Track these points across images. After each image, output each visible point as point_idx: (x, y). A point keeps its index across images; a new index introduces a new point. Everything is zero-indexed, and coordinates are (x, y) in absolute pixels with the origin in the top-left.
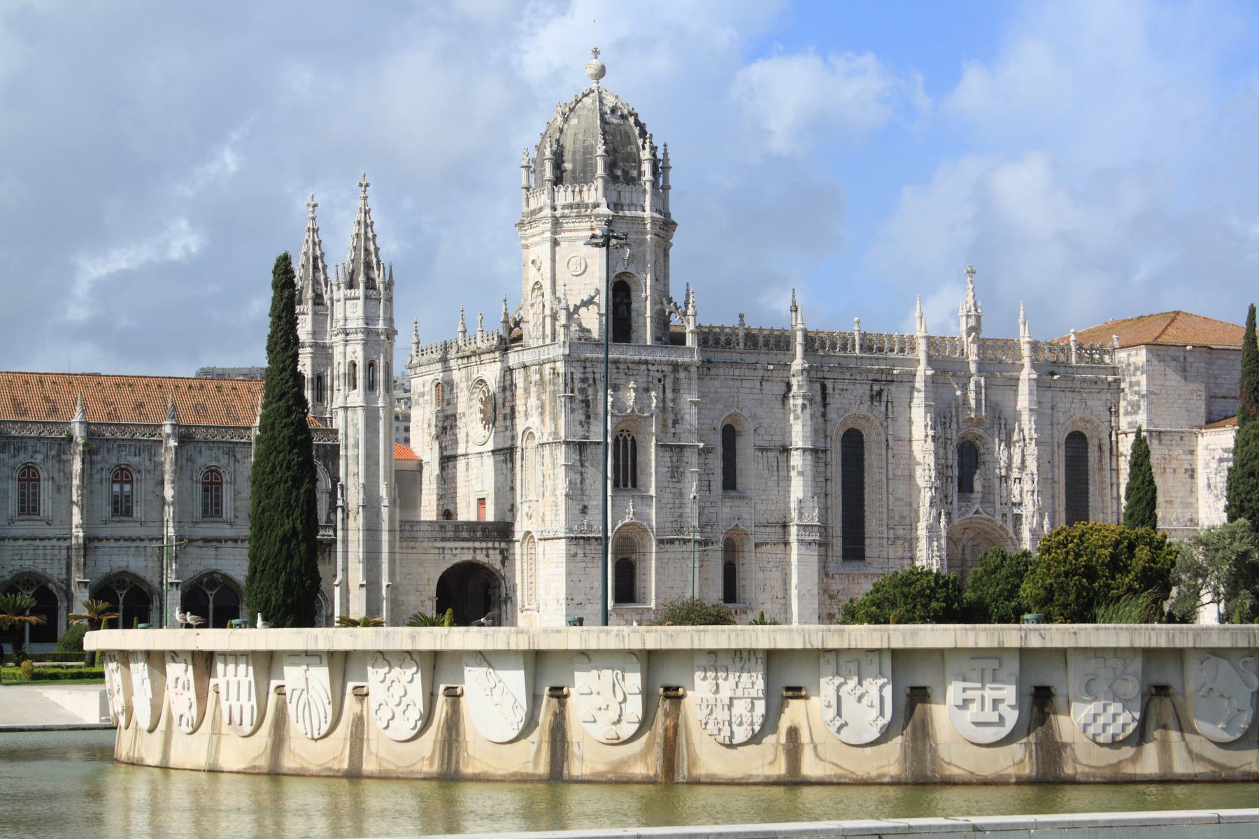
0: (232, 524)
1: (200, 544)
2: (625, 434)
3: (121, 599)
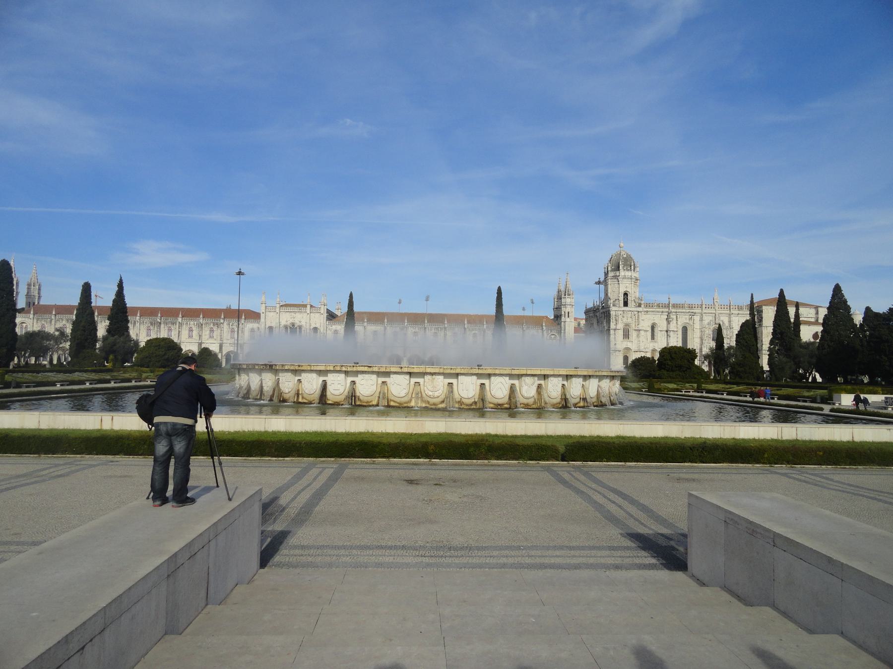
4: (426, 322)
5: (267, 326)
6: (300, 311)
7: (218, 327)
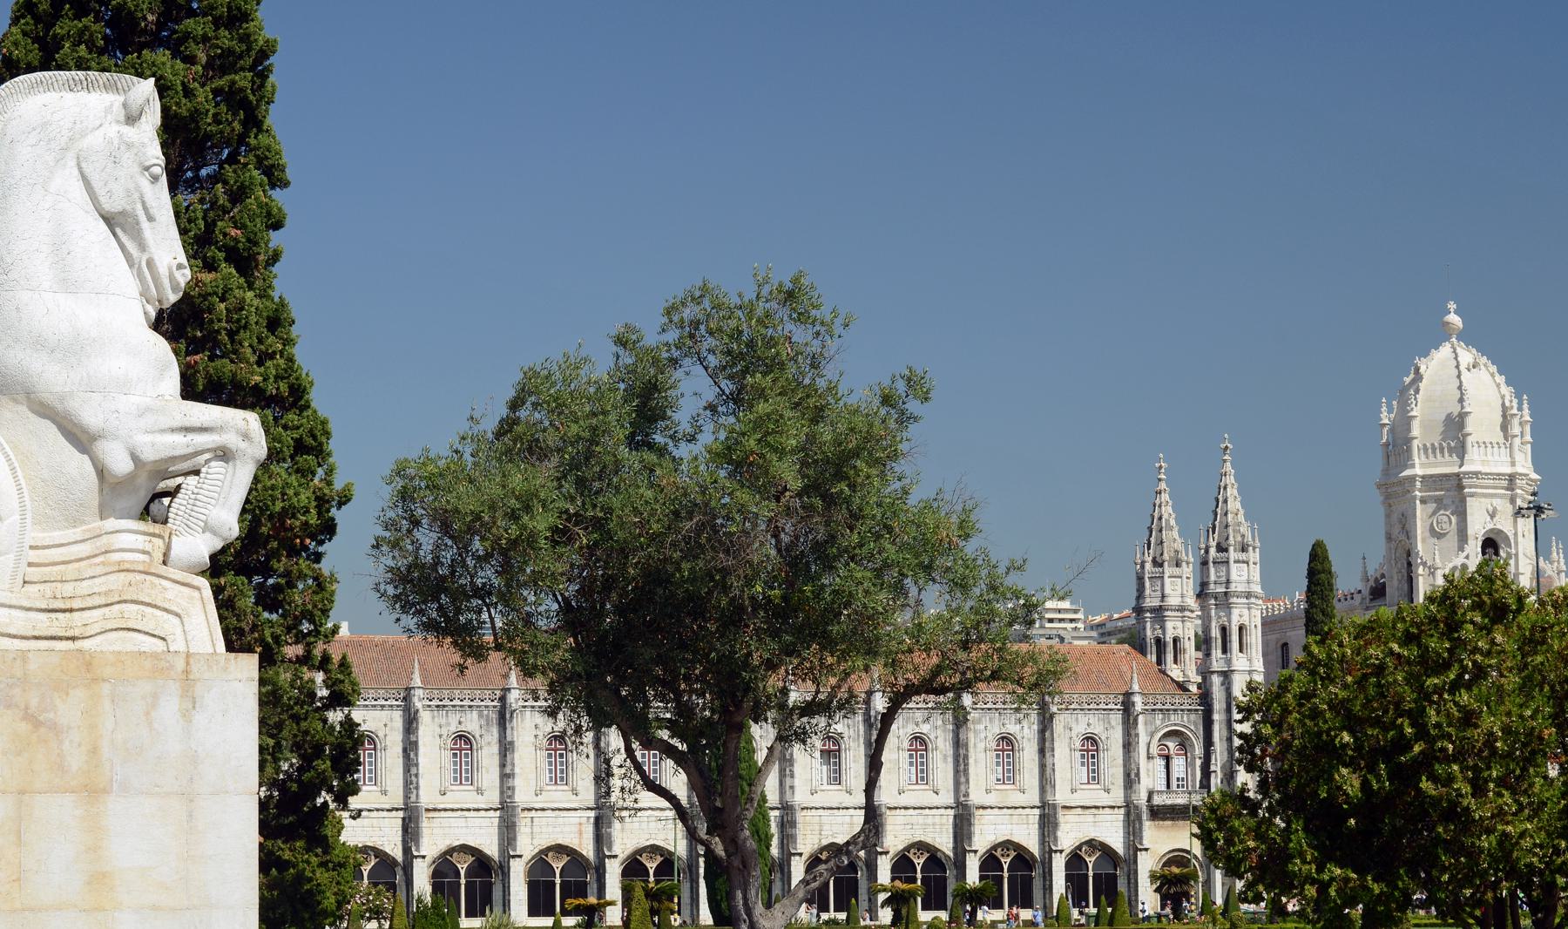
0: (1108, 791)
1: (1079, 811)
3: (1006, 867)
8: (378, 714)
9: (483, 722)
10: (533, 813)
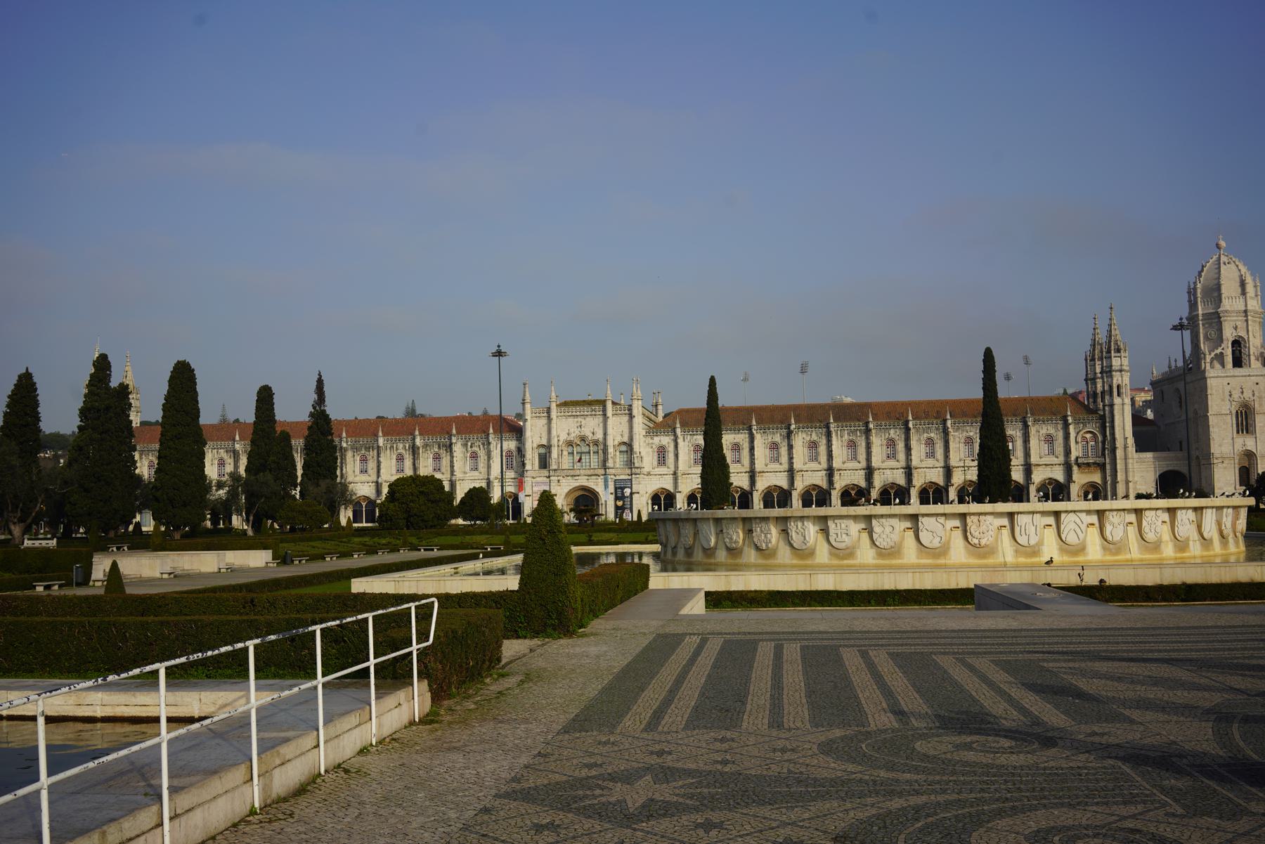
0: (1057, 457)
1: (1044, 466)
2: (1241, 409)
4: (832, 421)
5: (535, 445)
6: (593, 413)
7: (446, 450)
8: (739, 436)
9: (782, 437)
10: (803, 473)
